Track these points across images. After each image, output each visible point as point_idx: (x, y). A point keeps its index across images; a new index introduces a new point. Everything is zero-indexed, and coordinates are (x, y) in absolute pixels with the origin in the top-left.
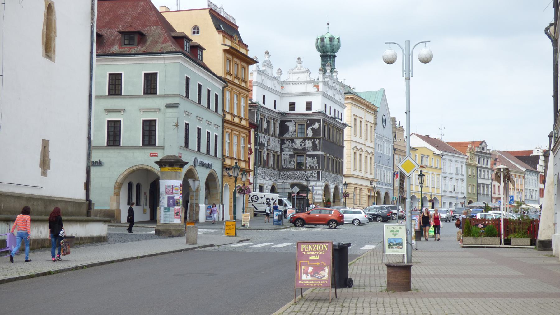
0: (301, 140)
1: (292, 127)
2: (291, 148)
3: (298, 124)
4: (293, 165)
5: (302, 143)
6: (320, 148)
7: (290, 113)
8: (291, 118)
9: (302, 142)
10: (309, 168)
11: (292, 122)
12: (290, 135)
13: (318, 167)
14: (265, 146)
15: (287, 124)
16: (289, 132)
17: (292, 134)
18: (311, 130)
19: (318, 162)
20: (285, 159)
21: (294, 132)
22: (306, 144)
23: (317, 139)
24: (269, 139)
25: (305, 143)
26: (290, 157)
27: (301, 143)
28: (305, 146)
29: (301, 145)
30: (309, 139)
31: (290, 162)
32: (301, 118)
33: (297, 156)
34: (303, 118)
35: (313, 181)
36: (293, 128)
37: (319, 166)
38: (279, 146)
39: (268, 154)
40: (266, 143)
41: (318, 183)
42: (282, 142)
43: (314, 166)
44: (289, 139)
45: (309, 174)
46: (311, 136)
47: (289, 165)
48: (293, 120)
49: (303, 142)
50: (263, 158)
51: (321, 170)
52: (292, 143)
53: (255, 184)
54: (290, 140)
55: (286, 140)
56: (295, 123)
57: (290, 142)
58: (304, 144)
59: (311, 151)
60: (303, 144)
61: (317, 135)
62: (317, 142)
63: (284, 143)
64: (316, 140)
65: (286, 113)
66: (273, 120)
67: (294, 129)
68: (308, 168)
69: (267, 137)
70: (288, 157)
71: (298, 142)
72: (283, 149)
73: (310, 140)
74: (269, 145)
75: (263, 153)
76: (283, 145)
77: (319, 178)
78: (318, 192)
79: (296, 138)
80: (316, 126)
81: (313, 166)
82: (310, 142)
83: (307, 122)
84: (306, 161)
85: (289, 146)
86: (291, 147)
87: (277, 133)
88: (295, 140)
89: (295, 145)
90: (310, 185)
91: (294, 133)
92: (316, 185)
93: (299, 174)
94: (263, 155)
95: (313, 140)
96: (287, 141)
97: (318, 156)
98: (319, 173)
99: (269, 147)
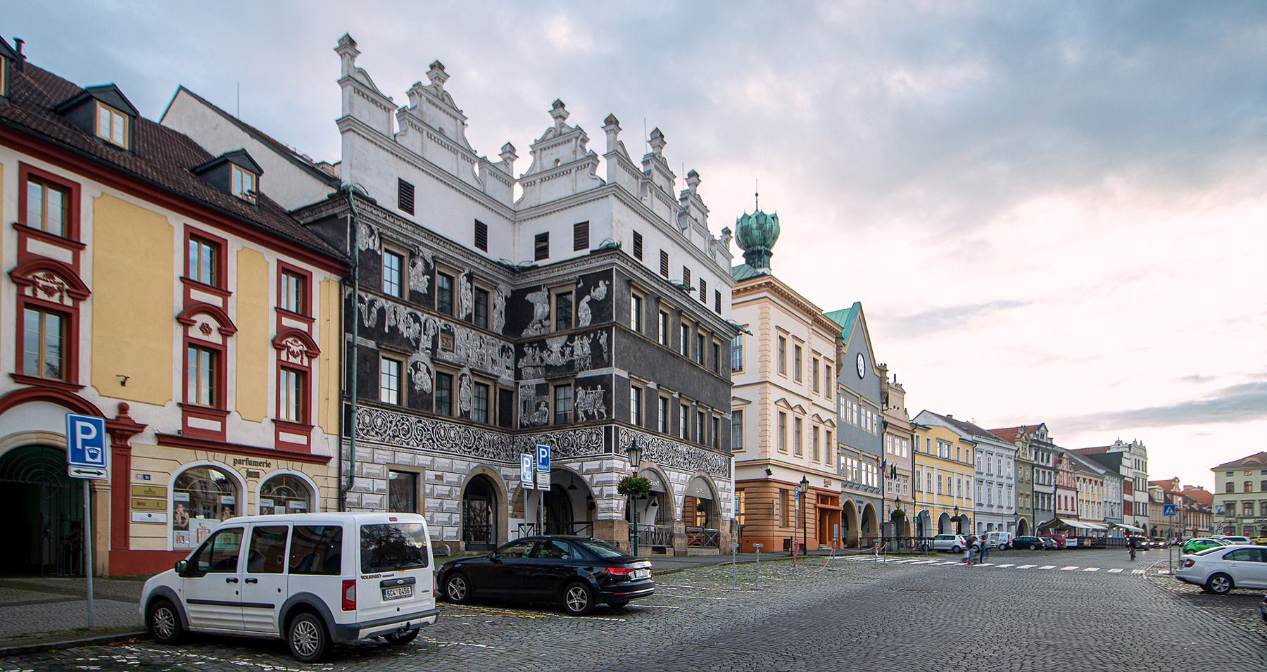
0: (565, 338)
1: (542, 306)
2: (540, 366)
3: (558, 296)
4: (545, 415)
5: (565, 348)
6: (610, 357)
7: (536, 267)
8: (538, 278)
9: (566, 345)
10: (582, 419)
11: (541, 290)
12: (536, 329)
13: (605, 416)
14: (421, 346)
15: (530, 297)
16: (534, 321)
17: (543, 326)
18: (586, 306)
19: (607, 401)
20: (525, 398)
21: (545, 320)
22: (575, 349)
23: (602, 329)
24: (449, 333)
25: (572, 347)
26: (537, 394)
27: (562, 347)
28: (572, 356)
29: (563, 354)
30: (584, 333)
31: (538, 405)
32: (561, 273)
33: (556, 387)
34: (566, 272)
35: (594, 458)
36: (544, 308)
37: (609, 411)
38: (510, 362)
39: (444, 379)
40: (424, 337)
41: (607, 464)
42: (520, 354)
43: (596, 414)
44: (535, 342)
45: (583, 439)
46: (588, 324)
47: (535, 417)
48: (544, 285)
49: (568, 343)
50: (411, 384)
51: (613, 421)
52: (541, 351)
53: (346, 466)
54: (535, 345)
55: (527, 345)
56: (547, 293)
57: (538, 348)
58: (570, 349)
59: (588, 369)
60: (568, 351)
61: (602, 320)
62: (603, 341)
63: (523, 354)
64: (601, 334)
65: (524, 269)
66: (470, 278)
67: (547, 307)
68: (580, 421)
69: (435, 323)
70: (533, 392)
71: (556, 345)
72: (520, 369)
73: (585, 337)
74: (444, 350)
75: (407, 368)
76: (521, 360)
77: (608, 450)
78: (607, 490)
79: (551, 336)
80: (600, 292)
81: (593, 413)
82: (586, 341)
83: (577, 283)
84: (575, 401)
85: (534, 360)
86: (540, 364)
87: (495, 324)
88: (548, 341)
89: (549, 356)
90: (587, 470)
91: (546, 323)
92: (599, 471)
93: (557, 440)
94: (410, 375)
95: (592, 336)
96: (530, 348)
97: (605, 381)
98: (608, 430)
99: (447, 356)
